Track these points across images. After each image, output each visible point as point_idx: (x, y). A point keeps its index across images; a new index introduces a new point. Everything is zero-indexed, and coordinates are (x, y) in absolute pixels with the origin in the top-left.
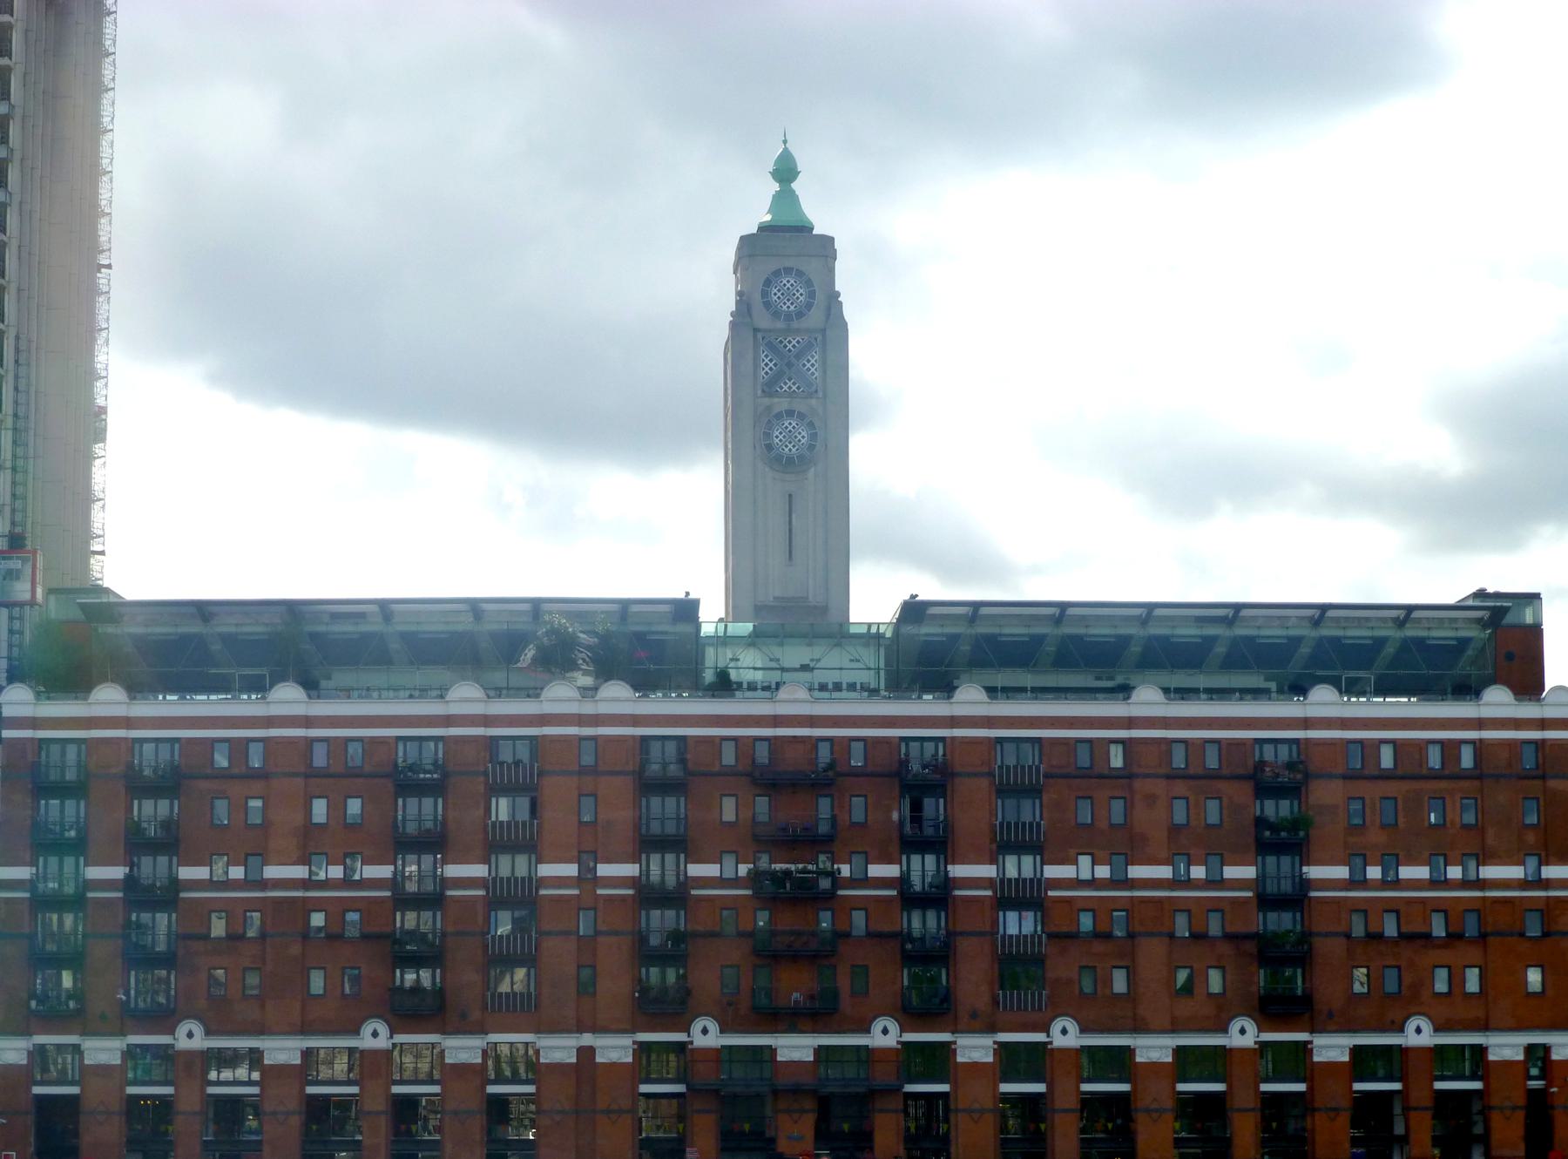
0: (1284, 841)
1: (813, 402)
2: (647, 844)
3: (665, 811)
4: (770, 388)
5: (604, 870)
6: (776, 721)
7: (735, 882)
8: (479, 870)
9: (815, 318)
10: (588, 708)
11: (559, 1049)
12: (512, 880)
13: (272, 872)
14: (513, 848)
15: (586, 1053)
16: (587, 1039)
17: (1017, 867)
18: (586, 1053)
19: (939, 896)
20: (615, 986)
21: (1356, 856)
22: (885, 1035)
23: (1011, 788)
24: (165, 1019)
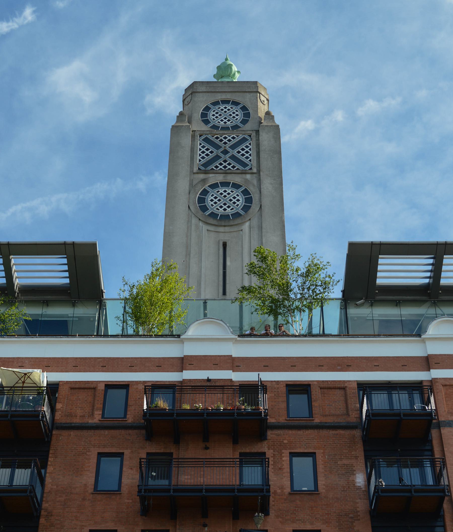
1: (248, 176)
4: (206, 168)
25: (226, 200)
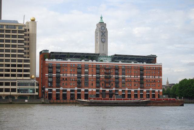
0: (142, 75)
2: (97, 74)
3: (98, 71)
4: (102, 35)
5: (93, 76)
6: (106, 64)
7: (103, 77)
8: (84, 75)
9: (105, 30)
10: (92, 62)
11: (90, 90)
12: (86, 76)
13: (67, 75)
14: (86, 74)
15: (92, 90)
16: (92, 89)
17: (124, 76)
18: (92, 90)
19: (118, 78)
20: (94, 85)
21: (147, 76)
22: (114, 89)
23: (123, 70)
24: (59, 87)
25: (103, 40)
